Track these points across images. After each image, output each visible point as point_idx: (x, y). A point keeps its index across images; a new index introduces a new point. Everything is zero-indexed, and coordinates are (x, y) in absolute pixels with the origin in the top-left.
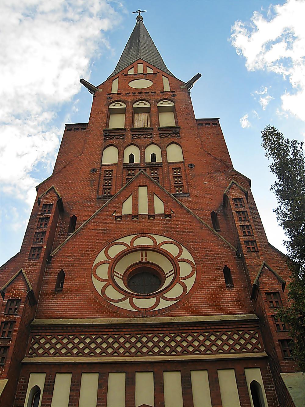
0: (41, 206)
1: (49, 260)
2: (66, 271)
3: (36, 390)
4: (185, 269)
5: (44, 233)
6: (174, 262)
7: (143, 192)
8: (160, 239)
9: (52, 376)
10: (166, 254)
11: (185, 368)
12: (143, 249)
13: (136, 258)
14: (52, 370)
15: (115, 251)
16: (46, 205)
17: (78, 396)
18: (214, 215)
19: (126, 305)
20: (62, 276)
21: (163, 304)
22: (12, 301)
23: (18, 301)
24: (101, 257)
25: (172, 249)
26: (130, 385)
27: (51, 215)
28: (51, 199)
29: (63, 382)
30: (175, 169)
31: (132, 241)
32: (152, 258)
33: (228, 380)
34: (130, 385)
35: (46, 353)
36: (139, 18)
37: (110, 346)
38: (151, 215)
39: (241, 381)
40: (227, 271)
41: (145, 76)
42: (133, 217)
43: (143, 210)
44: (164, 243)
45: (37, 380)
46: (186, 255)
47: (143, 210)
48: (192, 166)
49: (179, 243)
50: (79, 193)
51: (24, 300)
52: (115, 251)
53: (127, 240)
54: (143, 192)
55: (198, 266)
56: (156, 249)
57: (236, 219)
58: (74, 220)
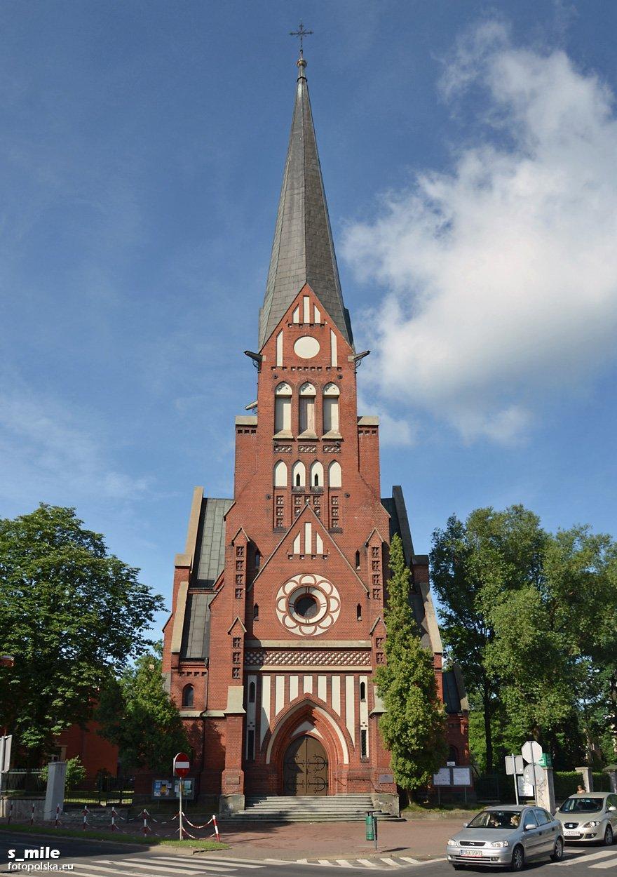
7: (308, 527)
8: (319, 578)
10: (322, 591)
13: (303, 592)
16: (239, 547)
18: (358, 554)
19: (296, 631)
21: (319, 631)
22: (235, 639)
23: (239, 639)
25: (326, 587)
26: (301, 682)
31: (300, 580)
33: (350, 680)
34: (301, 682)
39: (357, 681)
40: (359, 607)
41: (314, 329)
43: (308, 551)
46: (335, 593)
49: (333, 582)
50: (259, 524)
51: (243, 638)
53: (297, 578)
54: (308, 527)
55: (343, 601)
56: (316, 587)
57: (370, 568)
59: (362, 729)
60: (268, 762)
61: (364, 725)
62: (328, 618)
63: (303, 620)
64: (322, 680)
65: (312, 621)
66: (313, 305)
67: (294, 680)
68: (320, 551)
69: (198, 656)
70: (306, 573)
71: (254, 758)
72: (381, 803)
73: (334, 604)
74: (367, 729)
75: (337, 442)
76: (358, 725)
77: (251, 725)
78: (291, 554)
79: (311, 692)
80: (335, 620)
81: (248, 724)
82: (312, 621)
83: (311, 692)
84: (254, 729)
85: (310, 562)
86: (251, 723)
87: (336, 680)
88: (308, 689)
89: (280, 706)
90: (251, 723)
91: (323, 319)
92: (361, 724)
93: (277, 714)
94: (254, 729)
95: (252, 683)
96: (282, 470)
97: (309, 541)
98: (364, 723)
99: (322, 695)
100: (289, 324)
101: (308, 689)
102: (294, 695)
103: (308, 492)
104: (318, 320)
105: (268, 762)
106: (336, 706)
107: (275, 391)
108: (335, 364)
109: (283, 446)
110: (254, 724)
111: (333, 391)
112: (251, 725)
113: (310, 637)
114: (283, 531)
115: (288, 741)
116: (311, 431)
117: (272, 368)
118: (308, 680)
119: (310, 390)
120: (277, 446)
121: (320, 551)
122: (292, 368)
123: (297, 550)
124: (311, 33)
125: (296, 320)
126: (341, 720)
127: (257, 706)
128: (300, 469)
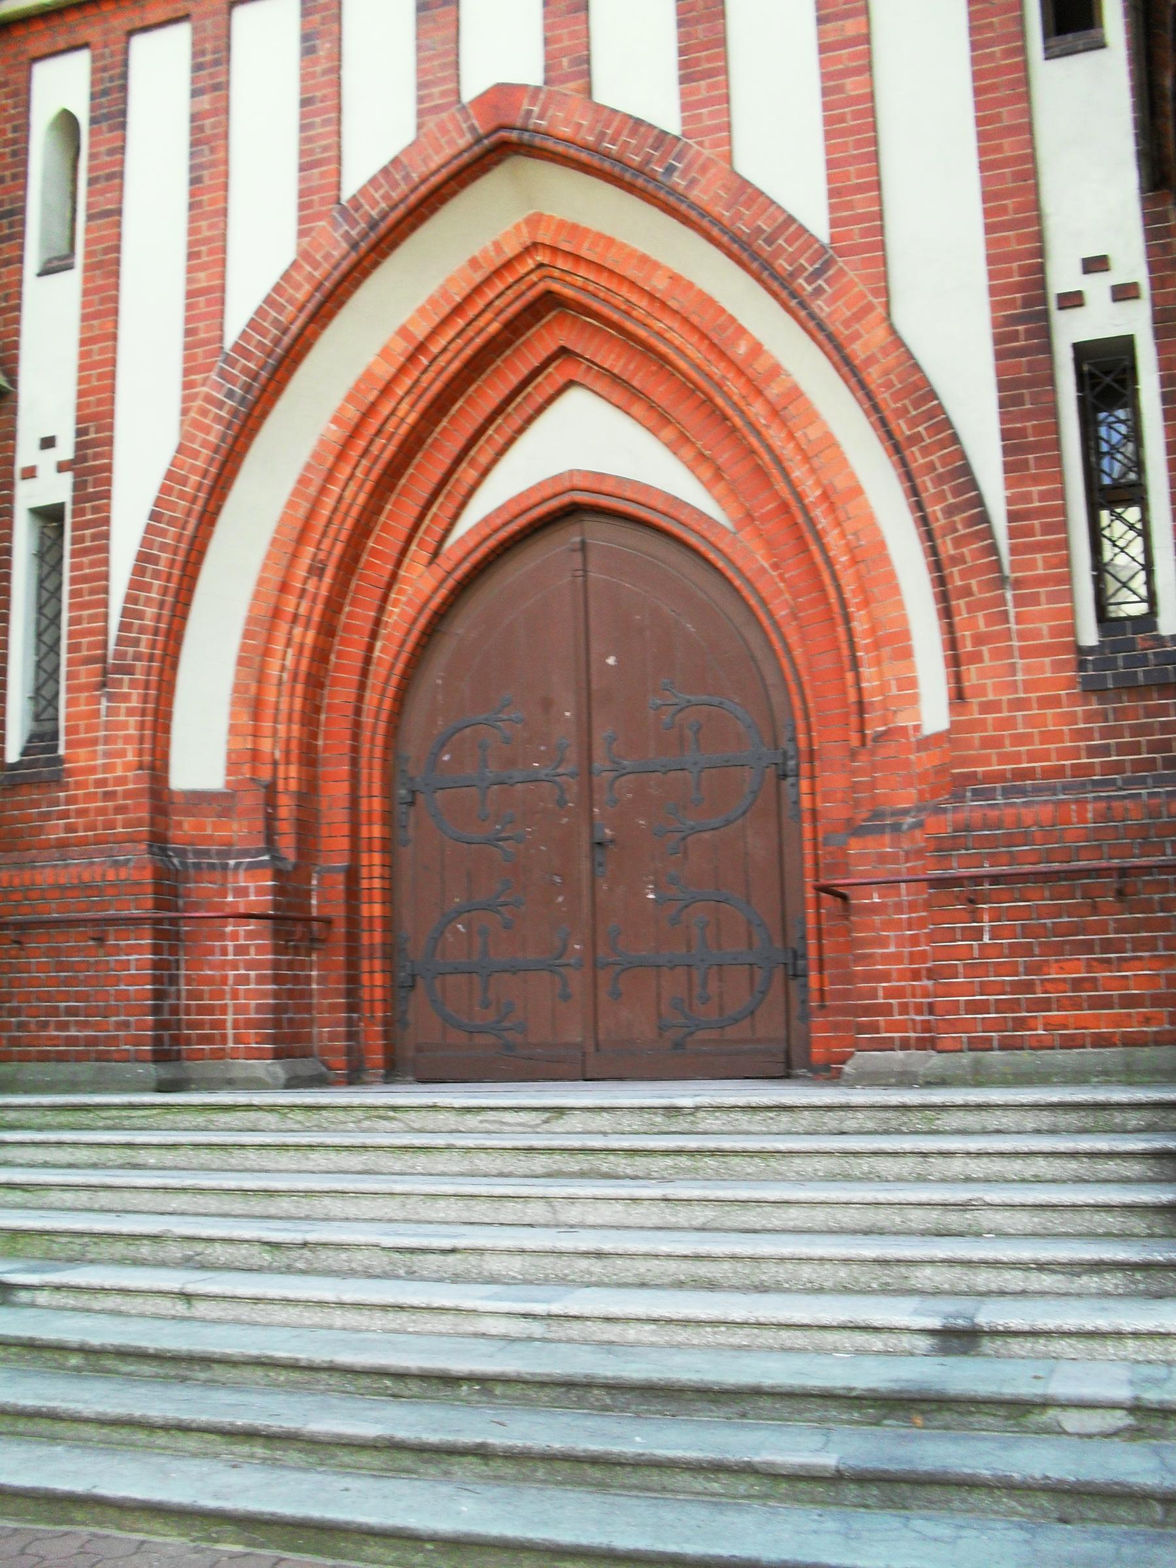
9: (113, 54)
17: (223, 110)
59: (1070, 330)
60: (200, 759)
61: (1097, 288)
71: (62, 751)
74: (1136, 321)
76: (1024, 306)
81: (26, 453)
86: (48, 443)
89: (264, 252)
92: (1063, 275)
93: (231, 335)
95: (67, 122)
98: (1095, 265)
105: (200, 759)
110: (65, 450)
115: (421, 583)
126: (830, 273)
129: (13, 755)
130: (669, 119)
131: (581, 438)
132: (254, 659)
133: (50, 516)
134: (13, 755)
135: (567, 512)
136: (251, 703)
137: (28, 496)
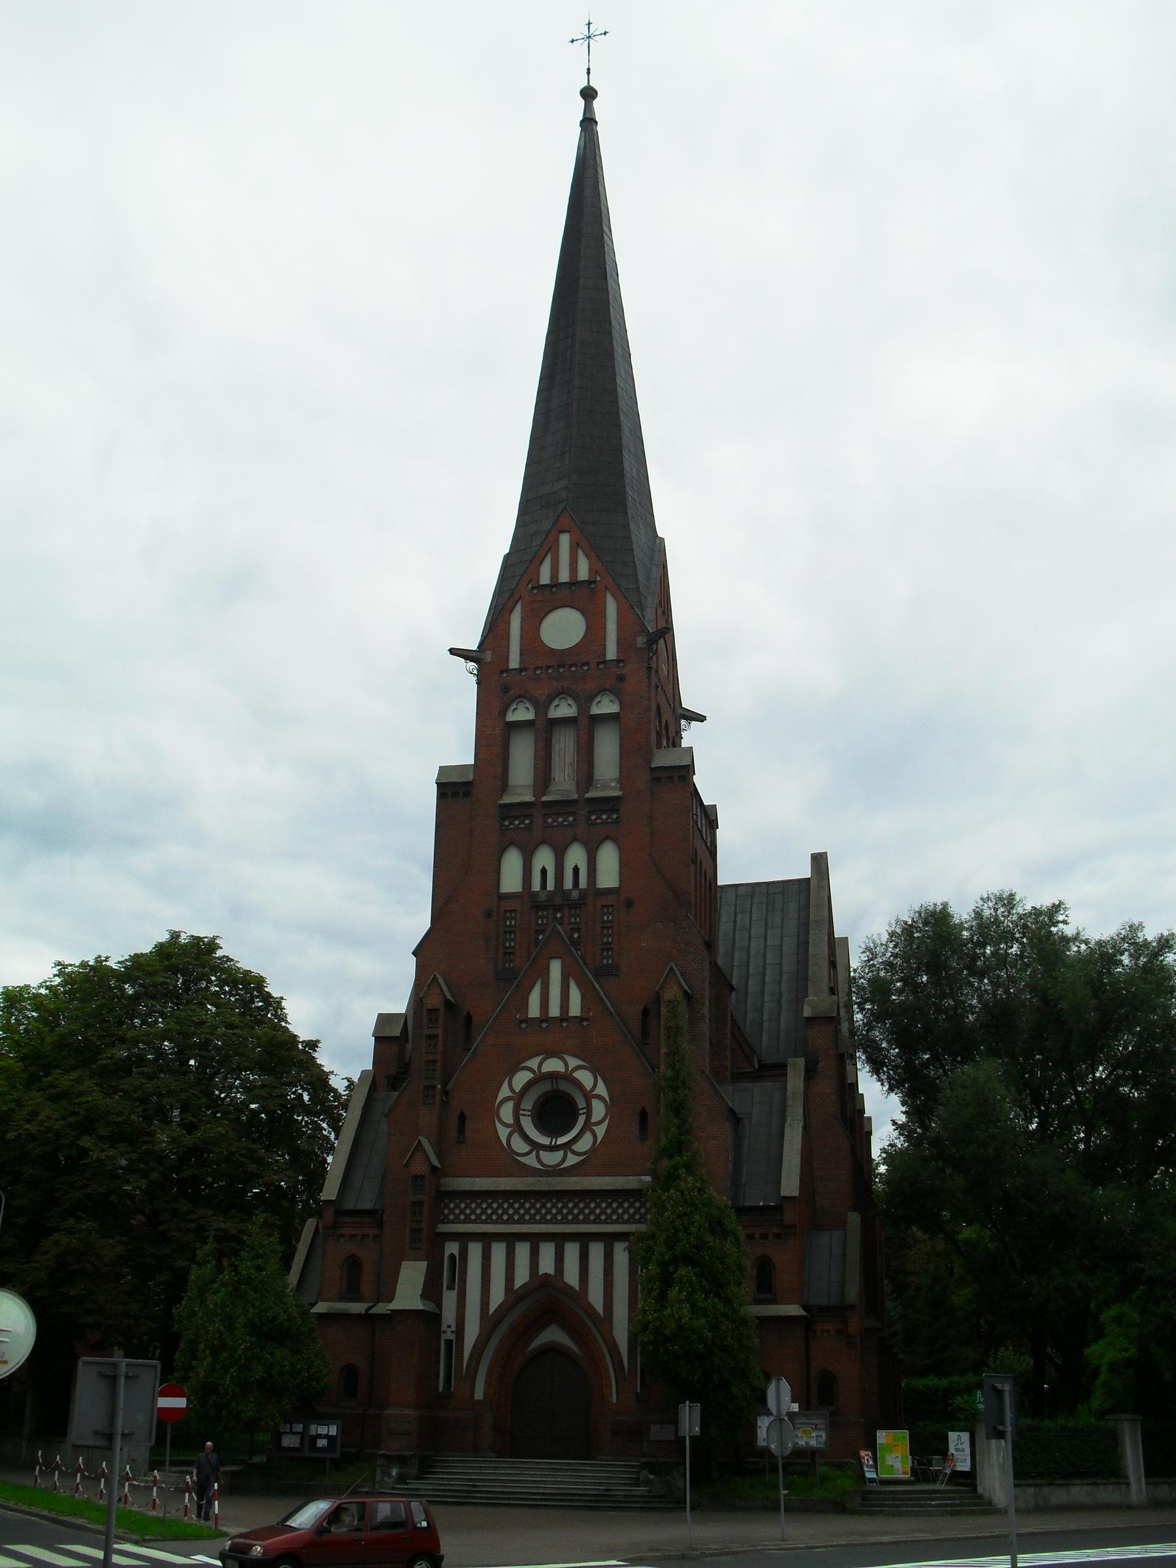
0: (425, 1013)
1: (445, 1104)
2: (467, 1113)
3: (452, 1257)
4: (599, 1110)
5: (435, 1062)
6: (588, 1096)
7: (556, 968)
8: (573, 1062)
11: (585, 1240)
12: (553, 1076)
13: (546, 1087)
14: (464, 1239)
15: (521, 1079)
19: (531, 1161)
20: (462, 1118)
21: (572, 1160)
22: (416, 1177)
24: (505, 1092)
27: (439, 1031)
28: (434, 1001)
29: (475, 1251)
30: (603, 906)
32: (564, 1086)
35: (456, 1221)
36: (589, 94)
37: (516, 1211)
38: (564, 1017)
40: (643, 1115)
42: (542, 1021)
43: (554, 1011)
44: (577, 1068)
45: (452, 1248)
47: (554, 1011)
48: (629, 903)
49: (594, 1071)
52: (521, 1079)
53: (533, 1063)
54: (556, 968)
55: (612, 1108)
56: (567, 1077)
58: (469, 1018)
60: (479, 1395)
62: (588, 1137)
63: (544, 1140)
64: (572, 1251)
65: (562, 1140)
66: (575, 547)
67: (523, 1251)
68: (575, 1010)
69: (367, 1205)
70: (551, 1054)
72: (651, 1476)
73: (599, 1110)
75: (610, 804)
77: (449, 1331)
78: (524, 1018)
79: (551, 1271)
80: (599, 1140)
81: (444, 1328)
82: (562, 1140)
83: (551, 1271)
84: (452, 1337)
85: (556, 1034)
87: (596, 1251)
88: (547, 1265)
89: (497, 1296)
90: (449, 1326)
91: (592, 571)
93: (491, 1312)
94: (452, 1337)
95: (452, 1257)
96: (512, 862)
97: (556, 993)
99: (572, 1277)
100: (533, 588)
101: (547, 1265)
102: (522, 1276)
103: (558, 901)
104: (583, 574)
105: (479, 1395)
106: (596, 1297)
107: (503, 713)
108: (611, 653)
109: (516, 817)
110: (453, 1328)
111: (606, 706)
112: (449, 1331)
113: (555, 1171)
114: (515, 977)
116: (564, 783)
117: (502, 672)
118: (547, 1252)
119: (564, 709)
120: (504, 819)
121: (575, 1010)
122: (536, 669)
123: (534, 1011)
124: (589, 24)
125: (545, 578)
127: (458, 1296)
128: (544, 858)
129: (441, 1389)
130: (577, 1288)
131: (553, 1334)
132: (489, 1374)
133: (449, 1343)
134: (441, 1389)
135: (552, 1349)
136: (488, 1383)
137: (444, 1337)
